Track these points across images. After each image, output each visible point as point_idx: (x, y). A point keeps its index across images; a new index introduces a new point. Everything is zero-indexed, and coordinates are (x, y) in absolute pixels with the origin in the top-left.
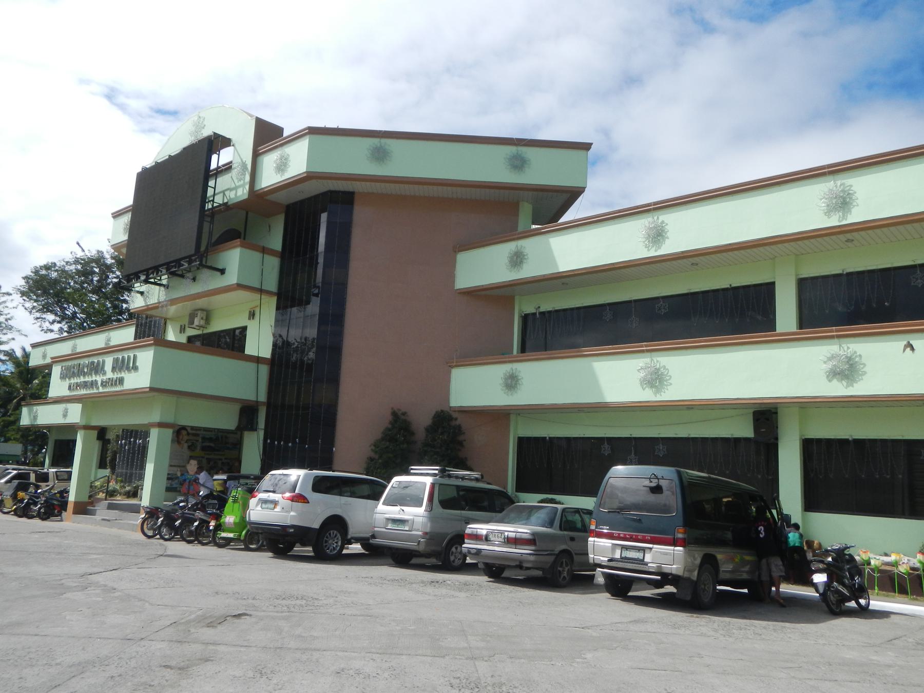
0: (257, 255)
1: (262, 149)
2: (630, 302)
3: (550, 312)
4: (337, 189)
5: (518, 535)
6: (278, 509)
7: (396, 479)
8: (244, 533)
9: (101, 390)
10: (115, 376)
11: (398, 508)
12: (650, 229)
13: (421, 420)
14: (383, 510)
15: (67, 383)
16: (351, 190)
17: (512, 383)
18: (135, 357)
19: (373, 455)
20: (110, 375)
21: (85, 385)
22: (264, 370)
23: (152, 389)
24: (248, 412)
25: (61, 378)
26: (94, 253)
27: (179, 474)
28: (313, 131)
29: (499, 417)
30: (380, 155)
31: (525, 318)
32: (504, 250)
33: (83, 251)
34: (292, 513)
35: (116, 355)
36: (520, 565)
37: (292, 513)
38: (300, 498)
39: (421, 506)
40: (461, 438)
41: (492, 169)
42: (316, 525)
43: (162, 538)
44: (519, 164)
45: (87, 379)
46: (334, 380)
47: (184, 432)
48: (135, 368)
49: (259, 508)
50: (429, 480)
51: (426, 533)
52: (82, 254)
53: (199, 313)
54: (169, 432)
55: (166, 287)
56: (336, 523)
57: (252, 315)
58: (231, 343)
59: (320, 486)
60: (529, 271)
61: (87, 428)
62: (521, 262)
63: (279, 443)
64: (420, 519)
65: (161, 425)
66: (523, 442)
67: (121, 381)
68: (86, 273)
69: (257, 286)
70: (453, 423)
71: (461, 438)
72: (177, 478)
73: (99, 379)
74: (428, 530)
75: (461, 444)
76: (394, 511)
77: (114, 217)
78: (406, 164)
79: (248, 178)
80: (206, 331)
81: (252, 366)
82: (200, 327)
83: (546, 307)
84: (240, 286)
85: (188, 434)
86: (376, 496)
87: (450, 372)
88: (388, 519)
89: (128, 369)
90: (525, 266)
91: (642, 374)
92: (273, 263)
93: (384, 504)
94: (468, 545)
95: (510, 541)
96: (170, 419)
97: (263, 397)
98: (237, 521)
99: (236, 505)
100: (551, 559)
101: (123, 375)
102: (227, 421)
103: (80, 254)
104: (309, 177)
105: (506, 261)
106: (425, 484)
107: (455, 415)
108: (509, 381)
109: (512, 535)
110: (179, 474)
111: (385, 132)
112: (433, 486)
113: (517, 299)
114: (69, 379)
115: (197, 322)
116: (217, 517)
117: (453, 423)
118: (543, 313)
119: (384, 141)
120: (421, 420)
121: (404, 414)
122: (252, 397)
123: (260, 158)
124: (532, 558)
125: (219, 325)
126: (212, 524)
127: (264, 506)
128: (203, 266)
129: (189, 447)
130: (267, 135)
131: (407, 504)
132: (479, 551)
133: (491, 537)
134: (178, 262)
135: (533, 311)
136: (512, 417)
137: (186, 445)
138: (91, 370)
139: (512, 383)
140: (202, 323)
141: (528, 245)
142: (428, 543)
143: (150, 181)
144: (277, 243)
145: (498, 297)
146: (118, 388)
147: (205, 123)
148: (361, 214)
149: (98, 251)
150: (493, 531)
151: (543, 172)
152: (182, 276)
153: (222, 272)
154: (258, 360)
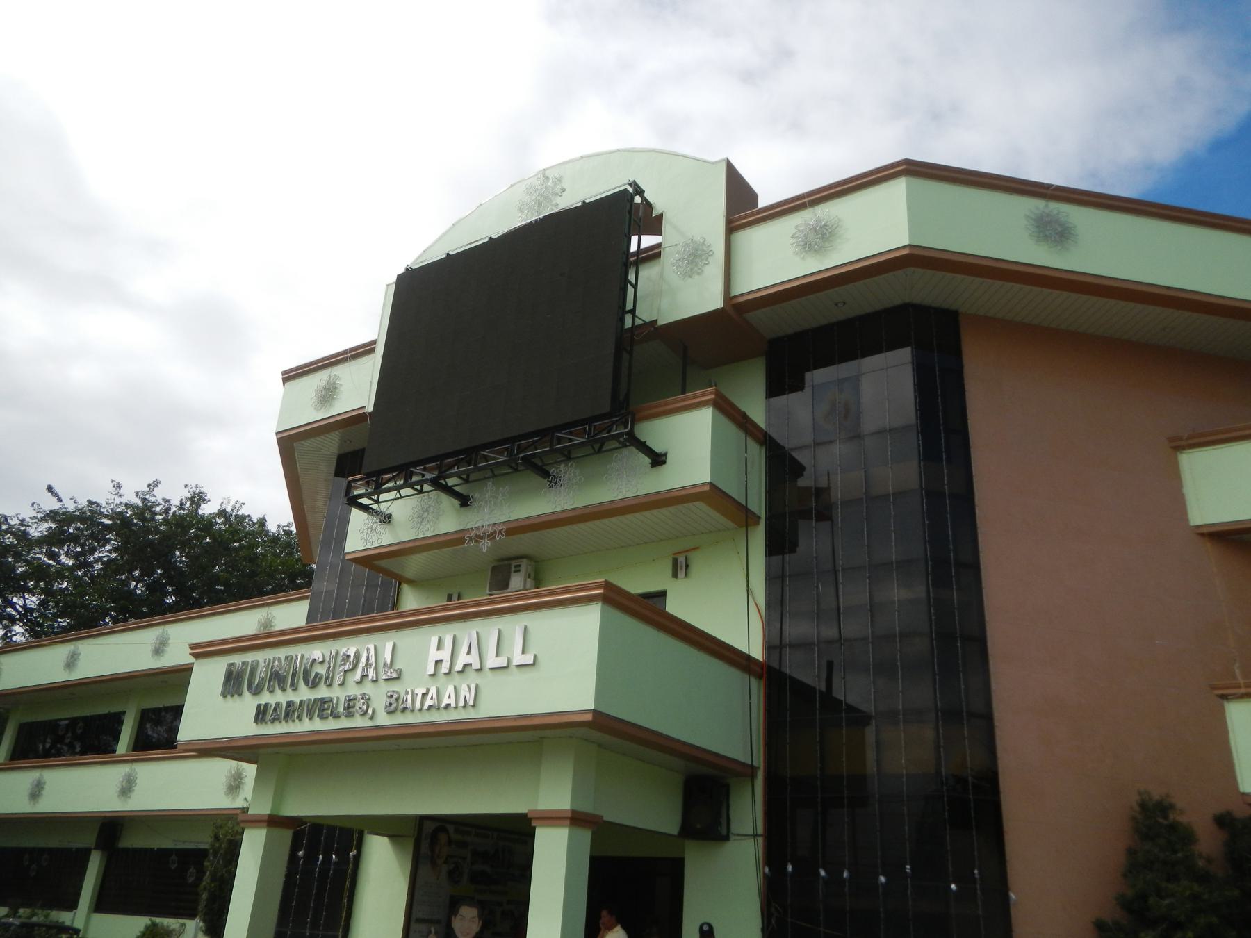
0: (732, 431)
9: (383, 719)
15: (248, 704)
16: (953, 308)
22: (757, 689)
25: (224, 695)
26: (83, 503)
33: (60, 500)
45: (322, 692)
47: (443, 838)
53: (524, 563)
54: (586, 836)
55: (465, 501)
57: (680, 567)
61: (273, 821)
65: (576, 819)
68: (53, 540)
79: (715, 270)
81: (734, 676)
85: (450, 842)
87: (1222, 712)
96: (587, 807)
97: (759, 761)
102: (652, 812)
103: (51, 504)
111: (1059, 188)
114: (256, 692)
119: (1055, 207)
123: (742, 237)
129: (450, 873)
147: (565, 185)
149: (91, 503)
152: (546, 474)
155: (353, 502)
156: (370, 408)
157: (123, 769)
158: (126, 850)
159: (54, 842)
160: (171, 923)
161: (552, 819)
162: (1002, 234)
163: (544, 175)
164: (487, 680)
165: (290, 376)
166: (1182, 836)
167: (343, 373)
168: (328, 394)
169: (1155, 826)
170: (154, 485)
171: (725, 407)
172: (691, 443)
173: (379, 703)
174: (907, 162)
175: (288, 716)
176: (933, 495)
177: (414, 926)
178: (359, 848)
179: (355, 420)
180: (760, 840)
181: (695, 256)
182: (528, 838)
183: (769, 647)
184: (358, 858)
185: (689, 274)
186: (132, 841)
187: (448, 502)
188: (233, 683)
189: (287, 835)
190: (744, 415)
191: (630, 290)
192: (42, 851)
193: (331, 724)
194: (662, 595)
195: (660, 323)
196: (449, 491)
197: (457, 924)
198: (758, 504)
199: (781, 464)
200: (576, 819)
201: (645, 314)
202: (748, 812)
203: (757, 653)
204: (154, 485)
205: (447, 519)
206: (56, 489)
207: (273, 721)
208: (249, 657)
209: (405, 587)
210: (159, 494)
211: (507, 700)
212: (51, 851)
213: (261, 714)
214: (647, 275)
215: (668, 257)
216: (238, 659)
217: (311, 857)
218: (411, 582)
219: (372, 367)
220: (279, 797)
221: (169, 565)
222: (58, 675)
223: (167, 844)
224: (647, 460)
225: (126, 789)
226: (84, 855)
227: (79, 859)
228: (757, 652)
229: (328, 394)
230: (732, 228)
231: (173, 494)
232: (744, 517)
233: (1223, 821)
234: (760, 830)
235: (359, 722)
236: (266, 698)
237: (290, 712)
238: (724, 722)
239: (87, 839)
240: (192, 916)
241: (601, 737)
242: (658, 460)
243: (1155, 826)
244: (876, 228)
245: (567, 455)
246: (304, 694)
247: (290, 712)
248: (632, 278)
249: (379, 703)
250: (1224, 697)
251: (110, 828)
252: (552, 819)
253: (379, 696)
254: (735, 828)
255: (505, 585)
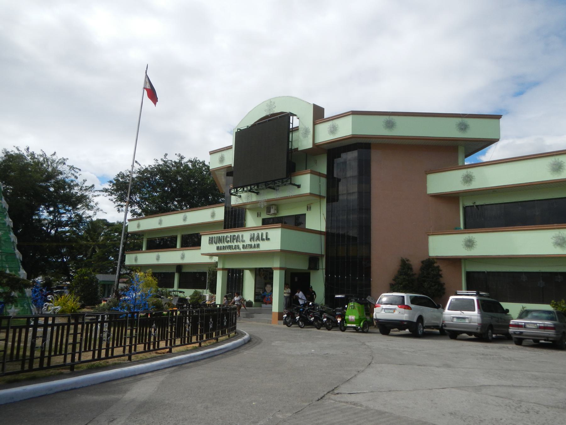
0: (317, 177)
1: (318, 121)
2: (534, 201)
3: (481, 205)
4: (362, 142)
5: (545, 325)
6: (396, 312)
7: (452, 298)
8: (362, 324)
9: (242, 250)
10: (253, 243)
11: (459, 312)
12: (554, 164)
13: (416, 264)
14: (449, 314)
17: (470, 244)
18: (267, 233)
19: (393, 282)
20: (248, 242)
21: (230, 247)
22: (323, 237)
23: (282, 251)
24: (313, 260)
25: (209, 243)
27: (261, 292)
28: (354, 113)
29: (455, 262)
30: (390, 125)
31: (465, 208)
32: (458, 175)
34: (406, 315)
35: (252, 232)
36: (547, 338)
37: (406, 315)
38: (408, 307)
39: (474, 310)
40: (440, 273)
41: (448, 130)
42: (415, 320)
43: (300, 327)
44: (463, 127)
45: (230, 244)
46: (368, 243)
47: (262, 270)
48: (268, 239)
49: (383, 312)
50: (475, 298)
51: (479, 324)
52: (140, 167)
53: (274, 206)
54: (283, 272)
55: (257, 193)
56: (420, 318)
57: (309, 208)
58: (297, 222)
59: (414, 301)
60: (475, 185)
61: (223, 269)
62: (471, 180)
63: (337, 276)
64: (476, 317)
65: (281, 269)
66: (468, 274)
67: (258, 246)
69: (317, 193)
70: (436, 265)
71: (440, 273)
72: (261, 294)
73: (241, 245)
74: (480, 322)
75: (441, 276)
76: (457, 313)
77: (210, 154)
78: (405, 129)
80: (277, 216)
82: (275, 214)
83: (478, 203)
84: (311, 194)
86: (444, 308)
88: (453, 317)
89: (263, 240)
90: (473, 183)
91: (553, 241)
92: (324, 180)
93: (449, 309)
94: (511, 330)
95: (540, 328)
96: (284, 266)
97: (324, 253)
98: (357, 318)
99: (354, 311)
100: (560, 336)
101: (258, 242)
102: (302, 265)
104: (353, 137)
105: (461, 179)
106: (473, 300)
107: (435, 260)
108: (468, 243)
109: (543, 325)
110: (261, 292)
111: (392, 112)
112: (478, 300)
113: (461, 198)
114: (216, 243)
115: (272, 211)
116: (343, 316)
117: (436, 265)
118: (477, 206)
119: (391, 117)
120: (416, 264)
121: (408, 260)
122: (320, 253)
124: (554, 336)
125: (284, 213)
126: (339, 320)
127: (386, 311)
128: (291, 184)
129: (264, 278)
130: (318, 113)
131: (462, 309)
132: (521, 333)
133: (528, 326)
134: (274, 181)
135: (472, 204)
136: (463, 261)
137: (263, 277)
138: (234, 239)
139: (470, 244)
140: (275, 212)
141: (474, 171)
142: (481, 329)
143: (243, 137)
144: (324, 170)
145: (451, 198)
146: (256, 250)
148: (376, 157)
150: (528, 323)
151: (476, 131)
152: (274, 189)
153: (299, 186)
154: (320, 233)
155: (231, 194)
156: (233, 166)
157: (181, 252)
158: (184, 273)
159: (164, 271)
160: (200, 290)
161: (276, 269)
162: (375, 129)
163: (270, 100)
164: (261, 243)
165: (212, 153)
166: (410, 268)
167: (225, 153)
168: (222, 160)
169: (405, 266)
170: (166, 155)
171: (313, 173)
172: (306, 182)
173: (241, 247)
174: (352, 111)
175: (223, 249)
176: (360, 193)
177: (257, 289)
178: (243, 273)
179: (229, 167)
180: (324, 270)
181: (306, 132)
182: (272, 273)
183: (327, 228)
184: (243, 275)
185: (305, 137)
186: (184, 270)
187: (253, 194)
188: (211, 241)
189: (227, 272)
190: (320, 173)
191: (290, 143)
192: (161, 273)
193: (232, 251)
194: (305, 214)
195: (299, 149)
196: (253, 192)
197: (267, 289)
198: (324, 193)
199: (332, 182)
200: (281, 269)
201: (295, 146)
202: (322, 264)
203: (323, 229)
204: (166, 155)
205: (254, 198)
206: (138, 162)
207: (221, 249)
208: (213, 236)
209: (247, 210)
210: (169, 158)
211: (265, 246)
212: (164, 273)
213: (218, 248)
214: (294, 136)
215: (301, 131)
216: (211, 236)
217: (232, 275)
218: (249, 209)
219: (232, 152)
220: (223, 264)
221: (176, 182)
222: (157, 226)
223: (196, 271)
224: (296, 187)
225: (183, 257)
226: (174, 274)
227: (172, 275)
228: (323, 229)
229: (222, 160)
230: (315, 124)
231: (173, 158)
232: (320, 197)
233: (423, 262)
234: (324, 267)
235: (238, 250)
236: (218, 245)
237: (224, 248)
238: (316, 247)
239: (174, 270)
240: (205, 288)
241: (283, 253)
242: (299, 186)
243: (405, 266)
244: (345, 129)
245: (279, 186)
246: (226, 244)
247: (224, 248)
248: (290, 140)
249: (241, 247)
250: (428, 235)
251: (179, 267)
252: (276, 269)
253: (241, 245)
254: (320, 267)
255: (270, 212)
